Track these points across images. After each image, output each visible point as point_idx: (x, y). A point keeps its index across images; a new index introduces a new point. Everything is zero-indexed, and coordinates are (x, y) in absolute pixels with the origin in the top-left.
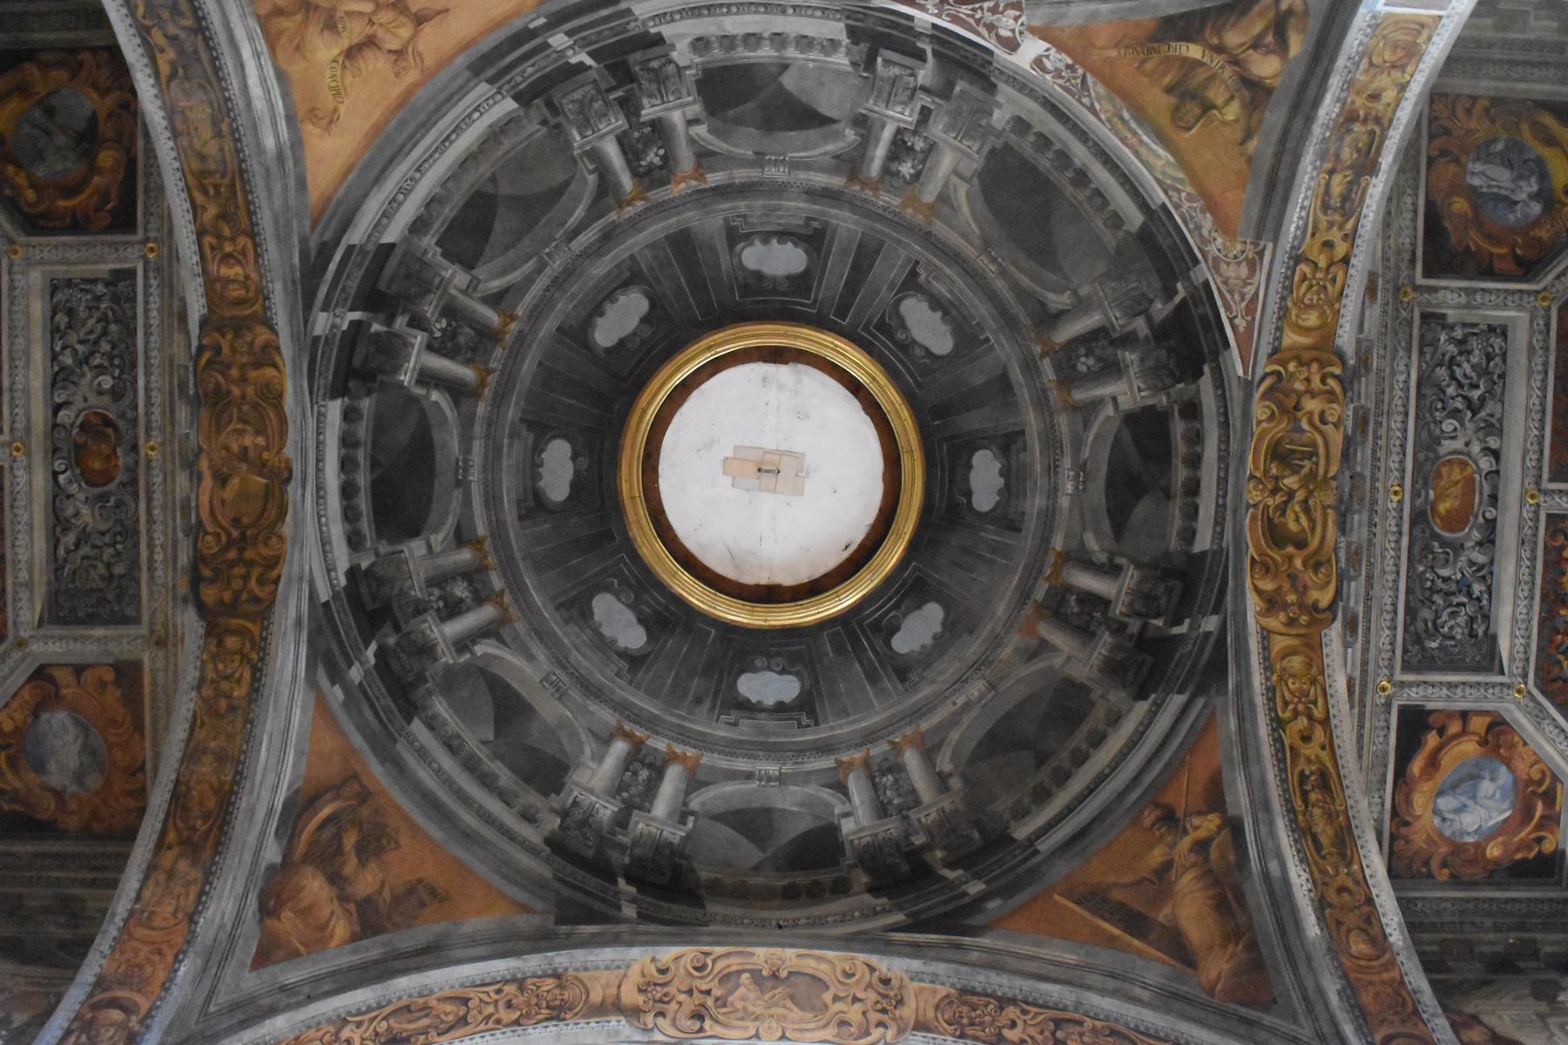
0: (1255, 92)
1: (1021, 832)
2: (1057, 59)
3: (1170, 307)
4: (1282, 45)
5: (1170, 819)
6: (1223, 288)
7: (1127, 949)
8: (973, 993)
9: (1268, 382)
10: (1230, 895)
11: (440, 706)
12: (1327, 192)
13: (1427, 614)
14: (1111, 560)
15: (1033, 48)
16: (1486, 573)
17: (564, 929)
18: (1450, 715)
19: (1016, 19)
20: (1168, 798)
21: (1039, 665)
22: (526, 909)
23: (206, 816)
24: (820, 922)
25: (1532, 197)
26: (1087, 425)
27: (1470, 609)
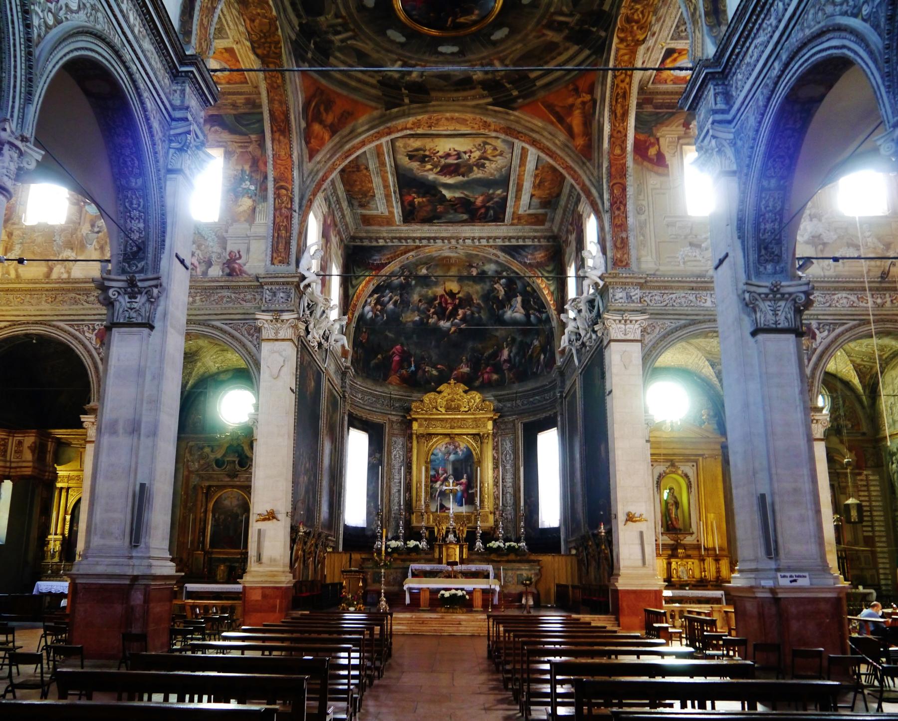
5: (577, 91)
7: (556, 127)
11: (338, 54)
17: (388, 112)
21: (543, 39)
22: (376, 109)
23: (283, 121)
24: (465, 99)
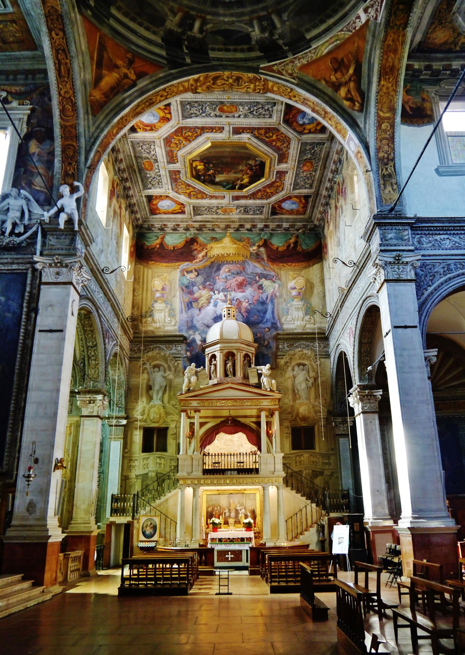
0: (337, 87)
1: (114, 11)
2: (358, 25)
3: (281, 44)
4: (347, 99)
5: (130, 63)
6: (285, 63)
7: (92, 65)
8: (62, 20)
9: (259, 78)
10: (116, 90)
12: (308, 100)
13: (196, 105)
14: (204, 31)
15: (364, 18)
16: (209, 115)
18: (170, 110)
19: (373, 16)
20: (136, 60)
25: (304, 123)
26: (246, 24)
27: (198, 113)
